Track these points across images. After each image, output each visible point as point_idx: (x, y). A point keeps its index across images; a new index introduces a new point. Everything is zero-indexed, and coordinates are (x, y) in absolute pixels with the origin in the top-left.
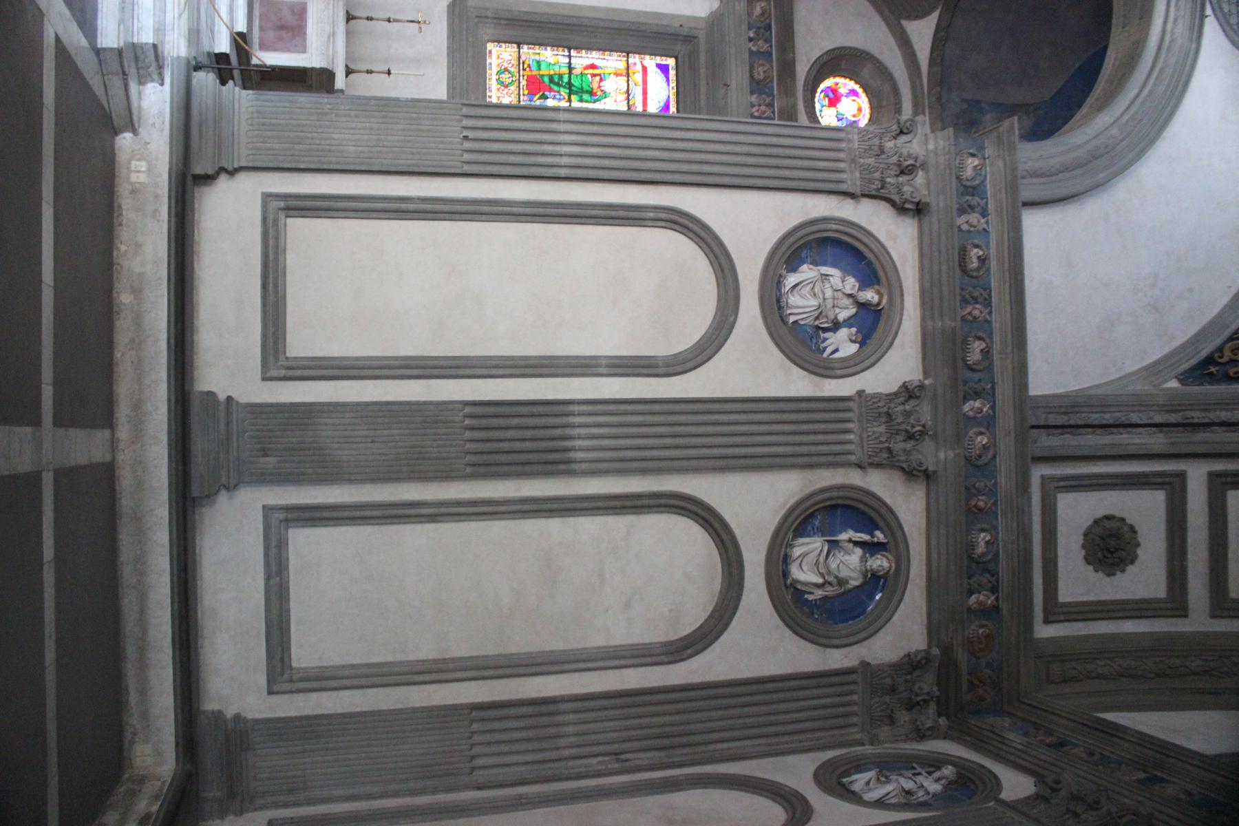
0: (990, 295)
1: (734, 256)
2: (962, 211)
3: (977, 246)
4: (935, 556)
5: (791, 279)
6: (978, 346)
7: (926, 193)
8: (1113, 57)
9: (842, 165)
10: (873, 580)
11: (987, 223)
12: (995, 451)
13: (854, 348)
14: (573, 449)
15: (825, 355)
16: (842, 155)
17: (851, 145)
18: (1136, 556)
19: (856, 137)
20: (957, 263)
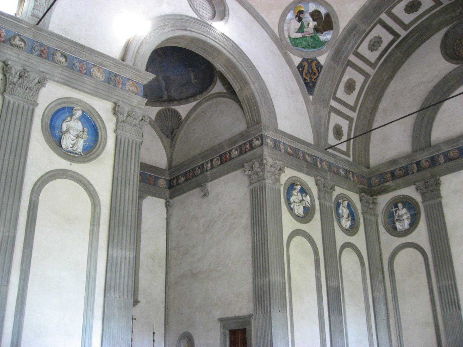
0: (297, 149)
1: (294, 229)
2: (280, 151)
3: (287, 149)
4: (345, 187)
5: (296, 212)
6: (308, 159)
7: (281, 162)
8: (219, 65)
9: (274, 187)
10: (349, 206)
11: (282, 142)
12: (319, 158)
13: (308, 197)
14: (336, 286)
15: (310, 206)
16: (272, 186)
17: (270, 183)
18: (341, 126)
19: (270, 181)
20: (292, 157)
